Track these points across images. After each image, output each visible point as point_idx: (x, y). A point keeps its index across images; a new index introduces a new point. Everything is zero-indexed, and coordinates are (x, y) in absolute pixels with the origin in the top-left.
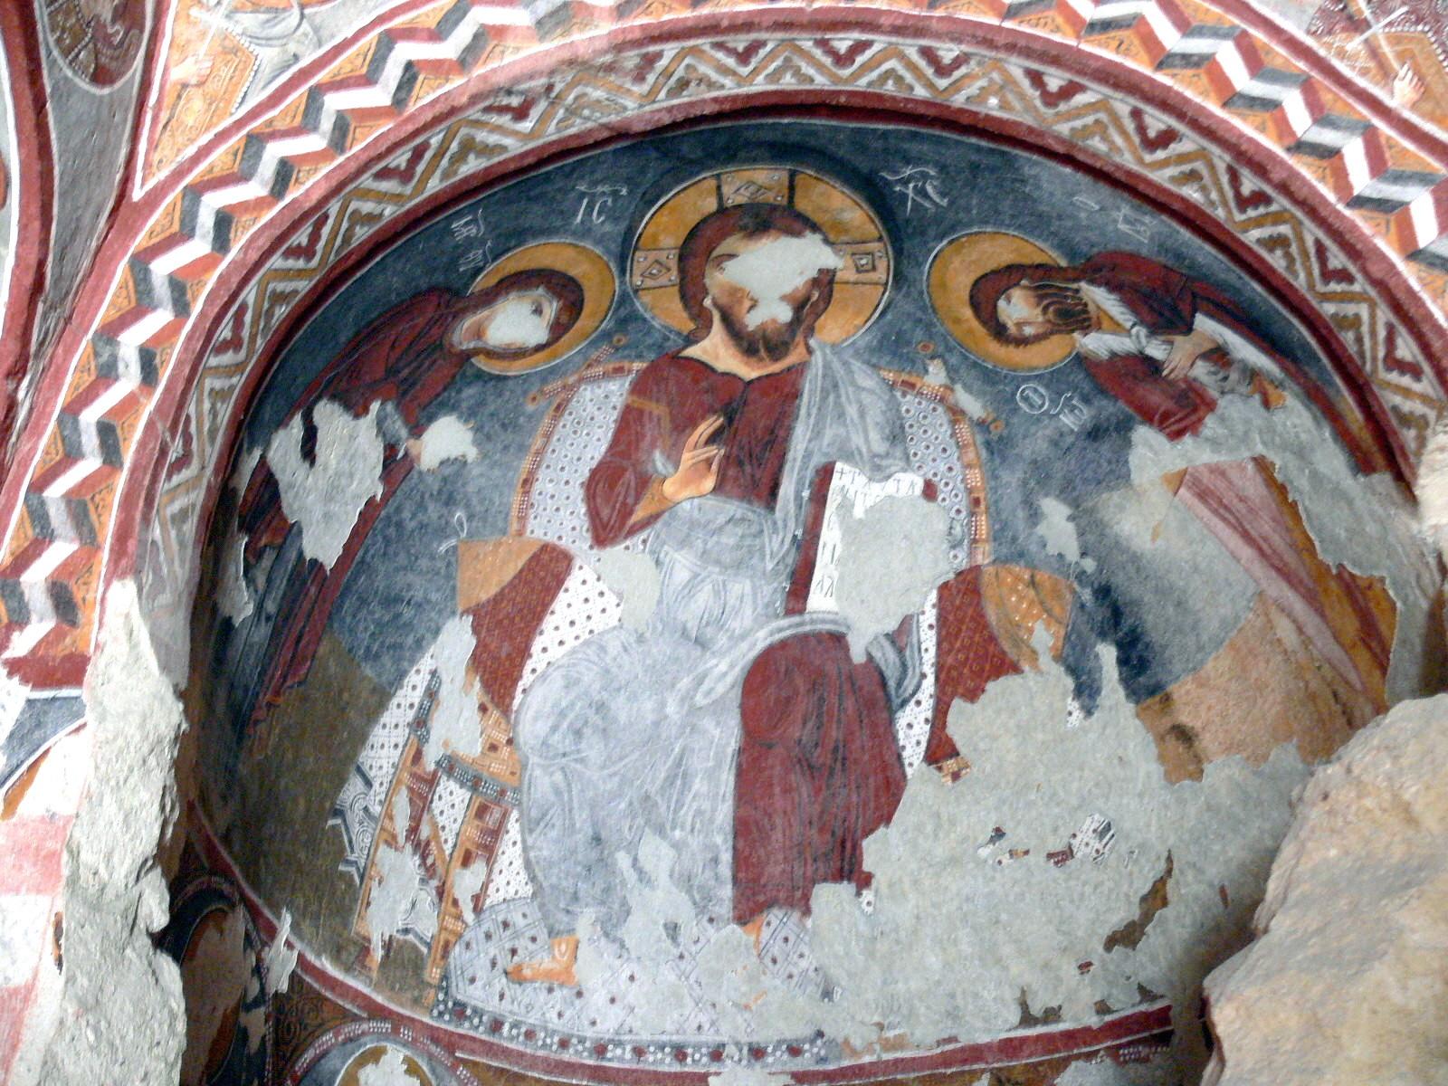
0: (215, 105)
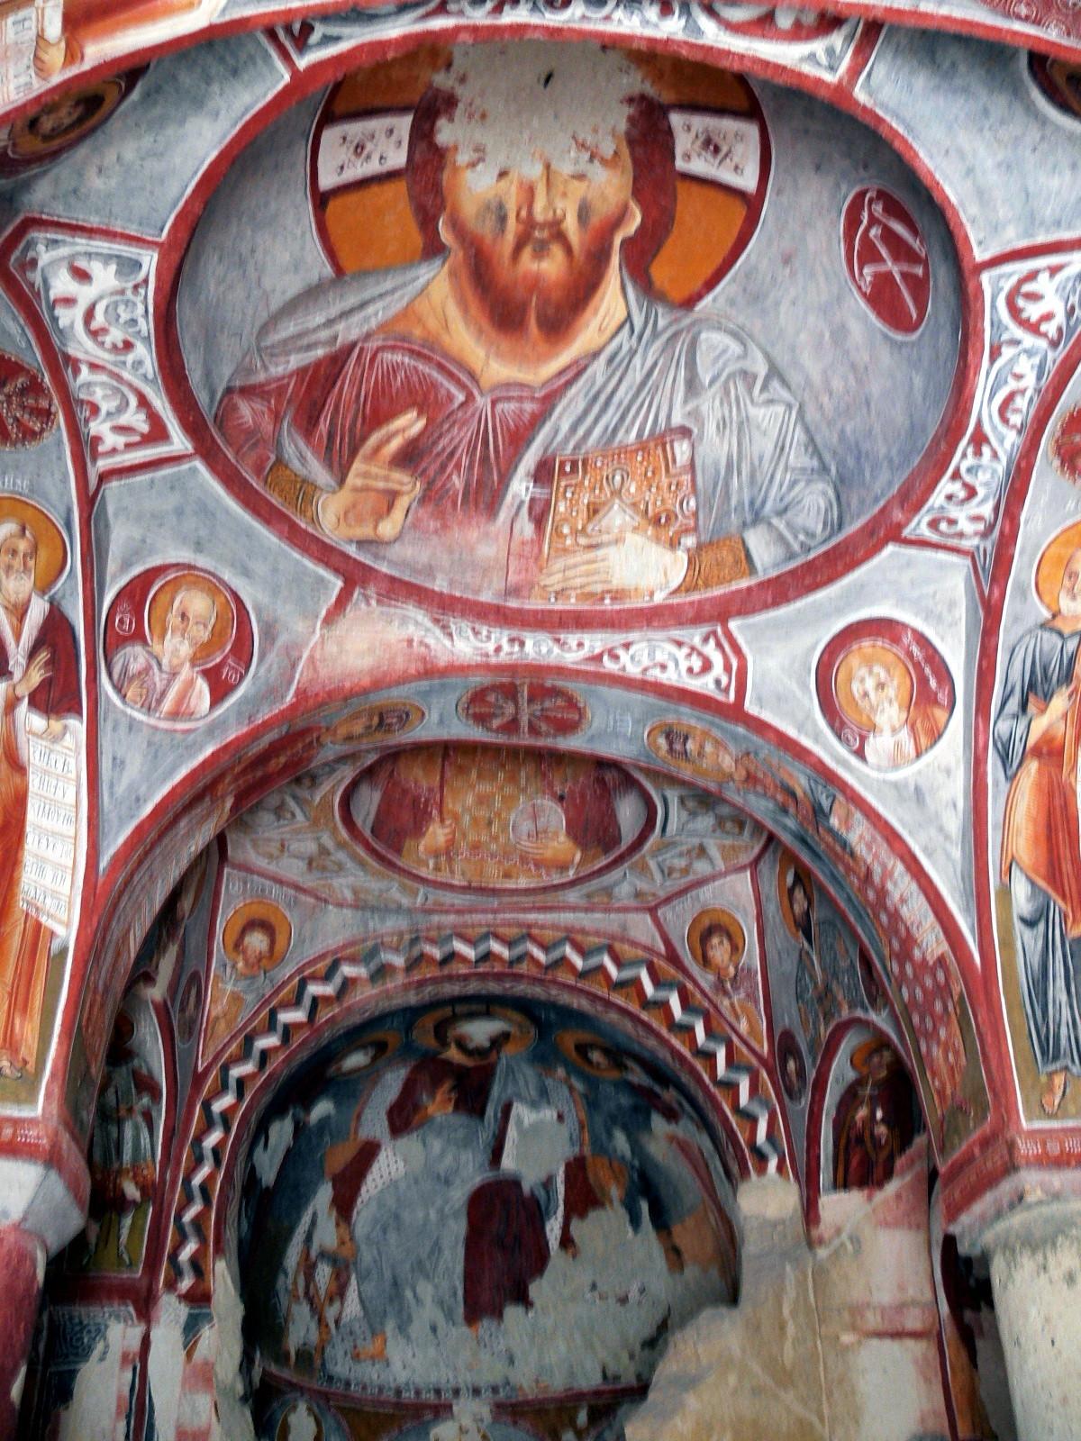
0: (229, 1024)
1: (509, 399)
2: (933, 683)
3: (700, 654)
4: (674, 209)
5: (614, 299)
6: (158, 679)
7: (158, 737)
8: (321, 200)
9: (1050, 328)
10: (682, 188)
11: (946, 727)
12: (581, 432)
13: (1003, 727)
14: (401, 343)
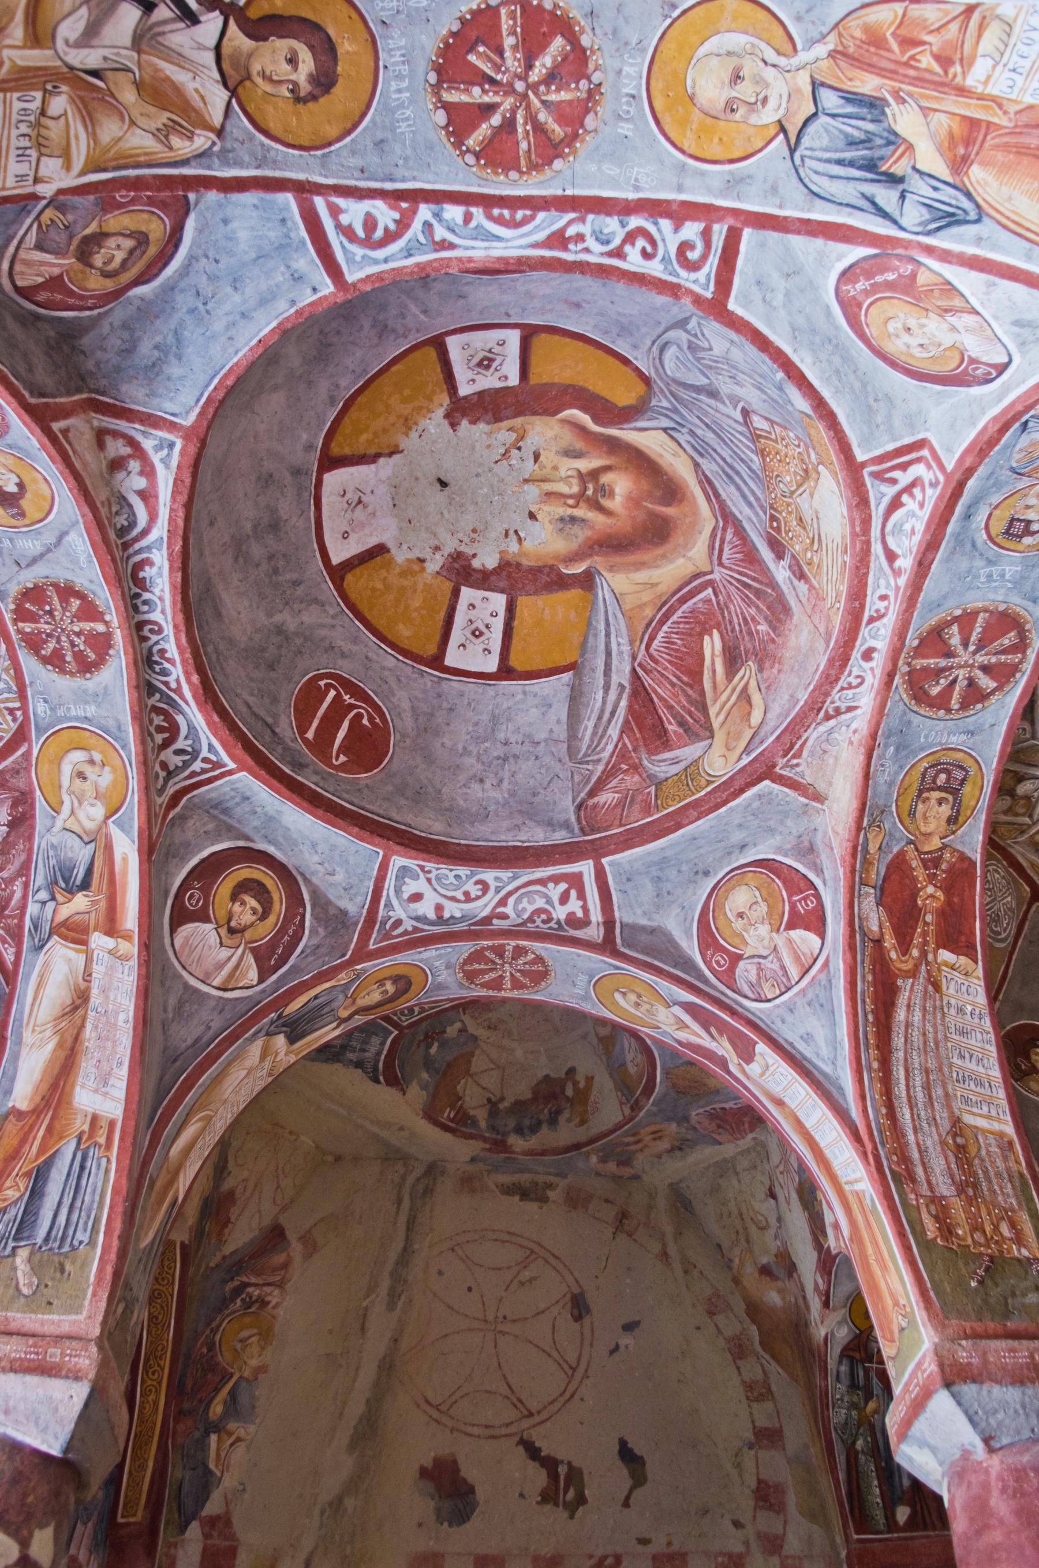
1: (721, 551)
2: (891, 277)
4: (562, 385)
5: (647, 437)
6: (771, 965)
7: (810, 995)
8: (506, 672)
10: (533, 380)
11: (940, 275)
12: (752, 499)
13: (912, 215)
14: (652, 628)
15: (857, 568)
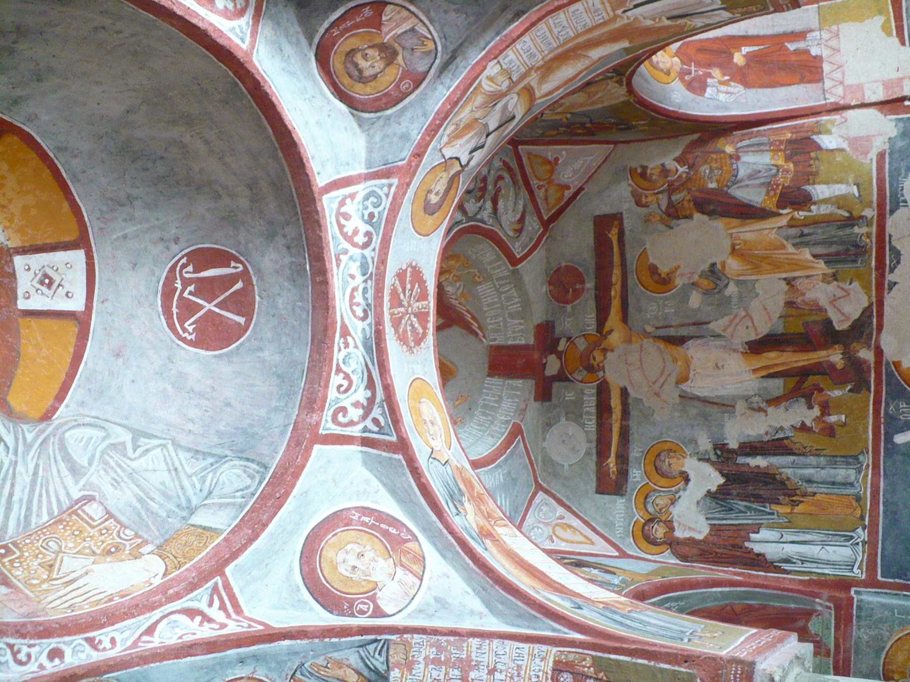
2: (393, 531)
3: (210, 620)
9: (360, 239)
15: (137, 606)
